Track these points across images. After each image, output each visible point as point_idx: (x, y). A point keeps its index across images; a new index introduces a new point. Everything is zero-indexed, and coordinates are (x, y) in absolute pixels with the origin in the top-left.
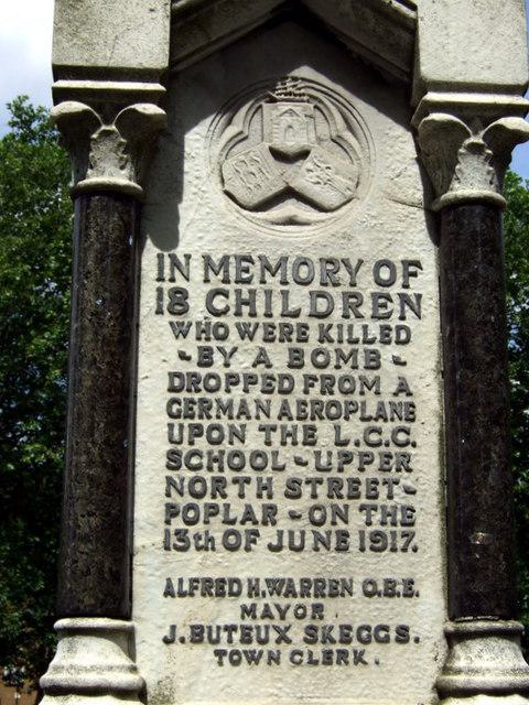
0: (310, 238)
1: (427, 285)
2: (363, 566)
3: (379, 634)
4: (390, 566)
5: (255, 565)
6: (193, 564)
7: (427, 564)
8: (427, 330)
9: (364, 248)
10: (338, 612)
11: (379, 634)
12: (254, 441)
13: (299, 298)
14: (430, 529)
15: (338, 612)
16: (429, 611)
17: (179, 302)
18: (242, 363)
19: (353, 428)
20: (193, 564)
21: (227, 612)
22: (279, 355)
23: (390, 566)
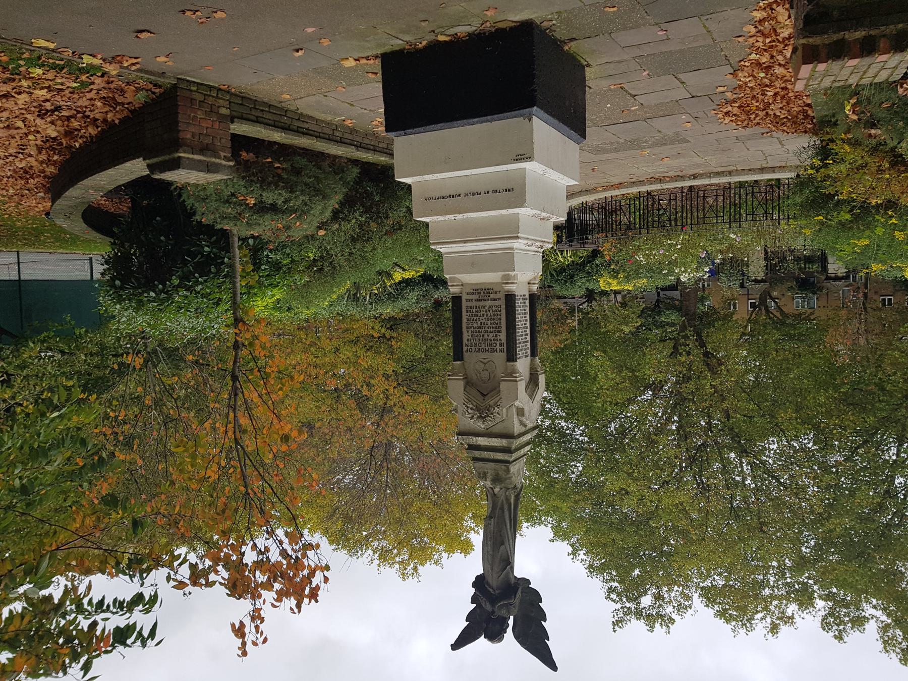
0: (482, 356)
1: (465, 348)
2: (473, 304)
3: (471, 294)
4: (470, 304)
5: (488, 303)
6: (497, 303)
7: (464, 304)
8: (465, 341)
9: (474, 354)
10: (477, 297)
11: (471, 294)
12: (489, 322)
13: (483, 345)
14: (464, 310)
15: (477, 297)
16: (465, 297)
17: (501, 345)
18: (491, 335)
19: (475, 325)
20: (497, 303)
21: (492, 296)
22: (486, 337)
23: (470, 304)
